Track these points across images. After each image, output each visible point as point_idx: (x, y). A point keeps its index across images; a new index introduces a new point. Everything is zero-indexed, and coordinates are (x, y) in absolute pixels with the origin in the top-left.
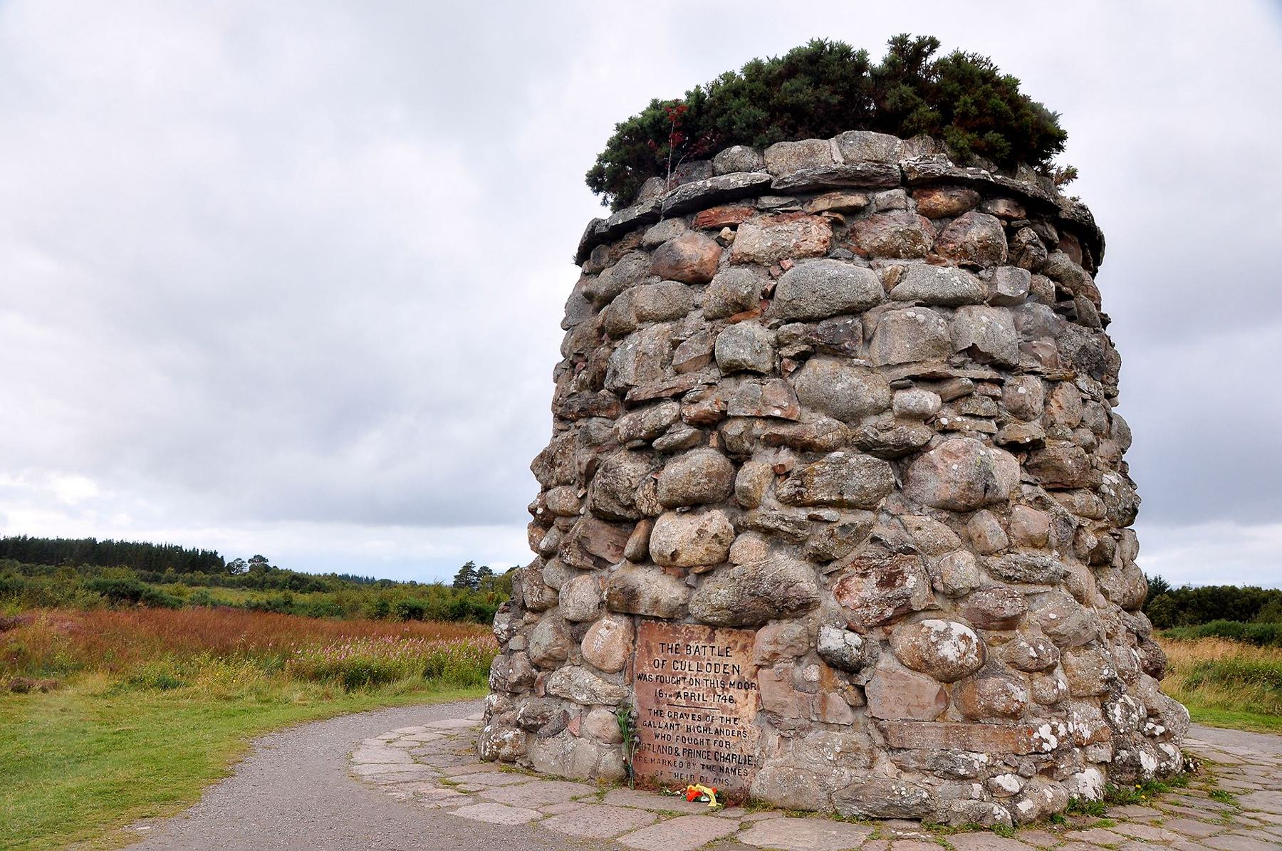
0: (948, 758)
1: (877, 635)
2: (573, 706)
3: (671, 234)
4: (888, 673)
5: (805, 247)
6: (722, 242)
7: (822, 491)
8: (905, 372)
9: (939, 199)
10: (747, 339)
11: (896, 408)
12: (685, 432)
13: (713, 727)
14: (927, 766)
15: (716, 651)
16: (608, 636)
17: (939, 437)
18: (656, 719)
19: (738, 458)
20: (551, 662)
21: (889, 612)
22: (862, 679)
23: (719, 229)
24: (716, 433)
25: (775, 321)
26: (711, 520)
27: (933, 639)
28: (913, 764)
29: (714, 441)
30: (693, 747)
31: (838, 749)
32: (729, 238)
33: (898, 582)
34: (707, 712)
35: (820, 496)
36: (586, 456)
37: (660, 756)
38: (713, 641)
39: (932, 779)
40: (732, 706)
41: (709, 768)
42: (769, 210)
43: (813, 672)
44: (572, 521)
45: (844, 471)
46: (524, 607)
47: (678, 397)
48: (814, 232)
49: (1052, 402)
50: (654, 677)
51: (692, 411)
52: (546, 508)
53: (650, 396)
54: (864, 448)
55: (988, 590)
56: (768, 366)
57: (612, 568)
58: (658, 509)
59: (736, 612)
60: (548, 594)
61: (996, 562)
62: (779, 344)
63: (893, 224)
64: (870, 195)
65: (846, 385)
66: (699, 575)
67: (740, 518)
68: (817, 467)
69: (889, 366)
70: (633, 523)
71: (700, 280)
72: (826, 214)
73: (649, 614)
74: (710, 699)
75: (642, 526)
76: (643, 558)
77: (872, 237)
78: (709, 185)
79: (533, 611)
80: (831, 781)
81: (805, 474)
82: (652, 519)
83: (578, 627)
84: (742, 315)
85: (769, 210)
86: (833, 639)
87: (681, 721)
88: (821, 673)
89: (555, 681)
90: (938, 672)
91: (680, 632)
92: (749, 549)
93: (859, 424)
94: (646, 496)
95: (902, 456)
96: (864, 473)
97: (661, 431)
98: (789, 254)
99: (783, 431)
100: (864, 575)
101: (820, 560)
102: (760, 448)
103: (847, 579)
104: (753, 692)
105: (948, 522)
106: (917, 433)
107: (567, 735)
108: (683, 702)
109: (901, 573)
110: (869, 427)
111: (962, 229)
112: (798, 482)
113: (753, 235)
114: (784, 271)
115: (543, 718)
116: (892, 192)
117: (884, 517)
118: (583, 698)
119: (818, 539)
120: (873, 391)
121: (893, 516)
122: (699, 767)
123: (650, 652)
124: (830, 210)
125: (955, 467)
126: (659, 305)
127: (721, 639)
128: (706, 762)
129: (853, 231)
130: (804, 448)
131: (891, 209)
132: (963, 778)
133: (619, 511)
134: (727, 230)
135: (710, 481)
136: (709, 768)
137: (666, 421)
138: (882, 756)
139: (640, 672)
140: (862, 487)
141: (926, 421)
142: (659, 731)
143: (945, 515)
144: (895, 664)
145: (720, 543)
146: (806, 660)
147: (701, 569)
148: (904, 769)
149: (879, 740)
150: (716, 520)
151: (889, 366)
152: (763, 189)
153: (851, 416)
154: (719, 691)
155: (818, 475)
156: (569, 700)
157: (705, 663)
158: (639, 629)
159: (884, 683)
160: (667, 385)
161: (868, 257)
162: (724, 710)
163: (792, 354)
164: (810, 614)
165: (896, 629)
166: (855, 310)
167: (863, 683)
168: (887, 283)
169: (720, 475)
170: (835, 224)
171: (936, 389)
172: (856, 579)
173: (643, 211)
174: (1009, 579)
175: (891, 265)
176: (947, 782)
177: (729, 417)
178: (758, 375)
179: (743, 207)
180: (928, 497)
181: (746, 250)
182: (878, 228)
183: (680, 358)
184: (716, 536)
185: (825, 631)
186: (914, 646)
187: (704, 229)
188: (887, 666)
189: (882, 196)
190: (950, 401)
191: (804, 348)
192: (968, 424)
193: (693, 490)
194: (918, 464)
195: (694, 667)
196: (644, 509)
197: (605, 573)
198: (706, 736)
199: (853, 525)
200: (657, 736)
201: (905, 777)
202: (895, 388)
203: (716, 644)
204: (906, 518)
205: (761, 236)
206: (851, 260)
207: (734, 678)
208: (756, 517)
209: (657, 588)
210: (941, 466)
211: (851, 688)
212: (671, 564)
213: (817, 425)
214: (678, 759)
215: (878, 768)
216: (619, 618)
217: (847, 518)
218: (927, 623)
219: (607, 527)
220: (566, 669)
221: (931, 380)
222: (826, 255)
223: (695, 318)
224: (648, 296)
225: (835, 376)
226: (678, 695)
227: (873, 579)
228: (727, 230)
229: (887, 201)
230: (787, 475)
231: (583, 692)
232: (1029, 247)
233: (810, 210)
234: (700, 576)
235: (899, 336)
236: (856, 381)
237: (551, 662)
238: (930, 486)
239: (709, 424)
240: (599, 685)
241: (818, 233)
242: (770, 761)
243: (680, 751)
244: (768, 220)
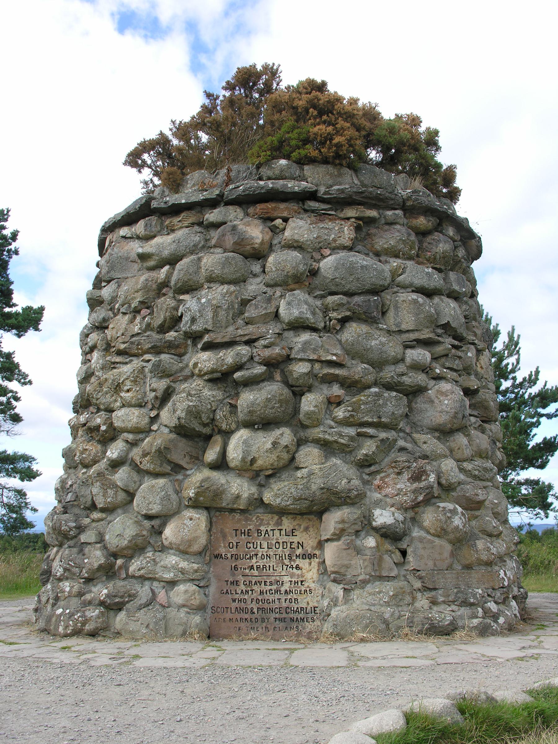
0: (462, 592)
1: (410, 514)
2: (155, 584)
3: (231, 217)
4: (421, 540)
5: (340, 242)
6: (274, 230)
7: (367, 415)
8: (412, 336)
9: (422, 221)
11: (408, 360)
12: (259, 369)
13: (283, 589)
14: (450, 599)
15: (283, 532)
16: (187, 526)
17: (432, 382)
18: (233, 588)
19: (298, 391)
20: (136, 548)
21: (421, 498)
22: (403, 545)
23: (272, 220)
24: (279, 371)
25: (319, 293)
26: (282, 435)
27: (449, 515)
28: (441, 599)
29: (278, 377)
30: (266, 606)
31: (391, 593)
32: (281, 227)
33: (423, 478)
34: (278, 578)
35: (365, 419)
36: (162, 385)
37: (238, 616)
38: (281, 525)
39: (454, 607)
40: (299, 572)
41: (280, 620)
42: (313, 211)
43: (371, 542)
44: (141, 436)
45: (381, 402)
46: (93, 507)
47: (250, 342)
48: (346, 232)
49: (478, 364)
50: (229, 555)
51: (267, 353)
52: (111, 425)
53: (226, 339)
54: (389, 387)
55: (469, 483)
56: (322, 325)
57: (189, 472)
58: (234, 426)
59: (312, 501)
60: (121, 496)
61: (467, 465)
62: (326, 310)
63: (397, 234)
64: (381, 211)
65: (377, 342)
66: (269, 477)
67: (302, 434)
68: (362, 398)
69: (400, 332)
70: (208, 438)
71: (258, 255)
72: (353, 220)
73: (230, 506)
74: (279, 569)
75: (218, 439)
76: (221, 464)
77: (384, 241)
78: (271, 186)
79: (103, 510)
80: (387, 616)
81: (354, 403)
82: (227, 434)
83: (157, 521)
84: (296, 286)
85: (313, 211)
86: (383, 517)
87: (255, 588)
88: (377, 542)
90: (451, 536)
91: (251, 520)
92: (309, 456)
93: (381, 370)
94: (224, 416)
95: (414, 393)
96: (392, 405)
97: (239, 367)
98: (328, 245)
99: (337, 371)
100: (399, 474)
101: (365, 464)
102: (316, 384)
103: (388, 476)
104: (315, 562)
105: (438, 439)
106: (420, 378)
107: (158, 606)
108: (256, 572)
109: (425, 471)
110: (389, 373)
111: (435, 243)
112: (349, 408)
113: (299, 228)
114: (324, 257)
115: (130, 596)
116: (397, 212)
117: (401, 434)
118: (169, 576)
119: (368, 448)
120: (393, 348)
121: (407, 434)
122: (272, 619)
123: (224, 536)
124: (357, 218)
125: (446, 402)
126: (226, 270)
127: (287, 524)
128: (277, 616)
129: (368, 235)
130: (353, 386)
131: (395, 223)
132: (472, 604)
133: (198, 428)
134: (278, 222)
135: (281, 406)
136: (280, 620)
137: (244, 359)
138: (419, 595)
139: (216, 552)
140: (393, 413)
141: (423, 371)
142: (237, 596)
143: (437, 434)
144: (423, 534)
145: (288, 452)
146: (363, 534)
147: (270, 472)
148: (434, 602)
149: (418, 584)
150: (285, 436)
151: (400, 332)
152: (312, 196)
153: (378, 364)
154: (287, 562)
155: (364, 404)
156: (154, 579)
157: (274, 542)
158: (214, 519)
159: (420, 545)
160: (240, 332)
161: (377, 254)
162: (292, 575)
163: (340, 317)
164: (363, 502)
165: (420, 509)
166: (375, 291)
167: (405, 546)
168: (395, 274)
169: (287, 402)
170: (358, 229)
171: (429, 349)
172: (393, 476)
173: (209, 197)
174: (475, 477)
175: (395, 263)
176: (463, 608)
177: (292, 359)
178: (314, 330)
179: (294, 206)
180: (427, 422)
181: (296, 237)
182: (388, 235)
183: (251, 312)
184: (286, 446)
185: (377, 512)
186: (437, 520)
187: (261, 218)
188: (419, 534)
189: (390, 213)
190: (435, 359)
191: (348, 313)
192: (450, 375)
193: (269, 413)
194: (420, 399)
195: (265, 545)
196: (224, 426)
197: (180, 477)
198: (277, 596)
199: (388, 439)
200: (234, 601)
201: (435, 608)
202: (406, 347)
203: (283, 527)
204: (415, 435)
205: (309, 229)
206: (367, 255)
207: (299, 551)
208: (317, 432)
209: (239, 487)
210: (436, 401)
211: (397, 550)
213: (358, 370)
214: (253, 617)
215: (418, 605)
216: (201, 511)
217: (383, 435)
218: (442, 505)
219: (184, 440)
220: (150, 554)
221: (426, 343)
222: (350, 249)
225: (369, 336)
226: (252, 567)
227: (406, 476)
228: (278, 222)
229: (393, 217)
230: (339, 404)
231: (170, 571)
232: (463, 260)
233: (342, 215)
234: (269, 477)
235: (406, 310)
236: (384, 340)
237: (136, 548)
238: (429, 414)
239: (276, 365)
240: (183, 564)
241: (347, 233)
242: (338, 608)
243: (255, 610)
244: (313, 219)
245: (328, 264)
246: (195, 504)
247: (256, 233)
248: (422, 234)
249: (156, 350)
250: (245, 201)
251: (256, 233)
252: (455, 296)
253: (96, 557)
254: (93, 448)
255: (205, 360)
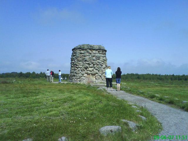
10: (94, 58)
19: (94, 65)
62: (96, 59)
71: (91, 54)
82: (88, 68)
83: (83, 75)
89: (82, 78)
92: (94, 70)
95: (102, 65)
101: (98, 71)
113: (94, 52)
119: (99, 70)
130: (98, 65)
150: (93, 68)
208: (95, 68)
212: (90, 71)
213: (98, 63)
223: (90, 56)
224: (88, 54)
235: (102, 59)
239: (92, 63)
245: (96, 55)
246: (86, 74)
247: (90, 52)
248: (103, 52)
249: (83, 61)
250: (90, 49)
251: (90, 52)
252: (105, 57)
253: (79, 77)
254: (77, 69)
255: (87, 62)
